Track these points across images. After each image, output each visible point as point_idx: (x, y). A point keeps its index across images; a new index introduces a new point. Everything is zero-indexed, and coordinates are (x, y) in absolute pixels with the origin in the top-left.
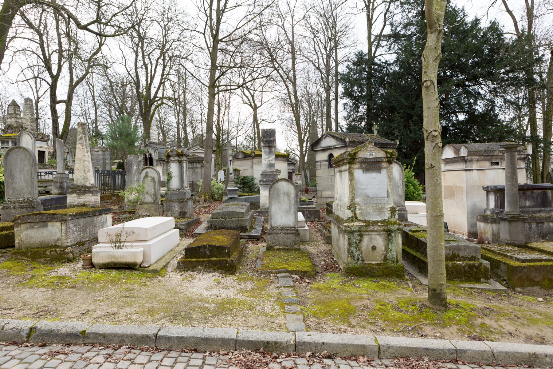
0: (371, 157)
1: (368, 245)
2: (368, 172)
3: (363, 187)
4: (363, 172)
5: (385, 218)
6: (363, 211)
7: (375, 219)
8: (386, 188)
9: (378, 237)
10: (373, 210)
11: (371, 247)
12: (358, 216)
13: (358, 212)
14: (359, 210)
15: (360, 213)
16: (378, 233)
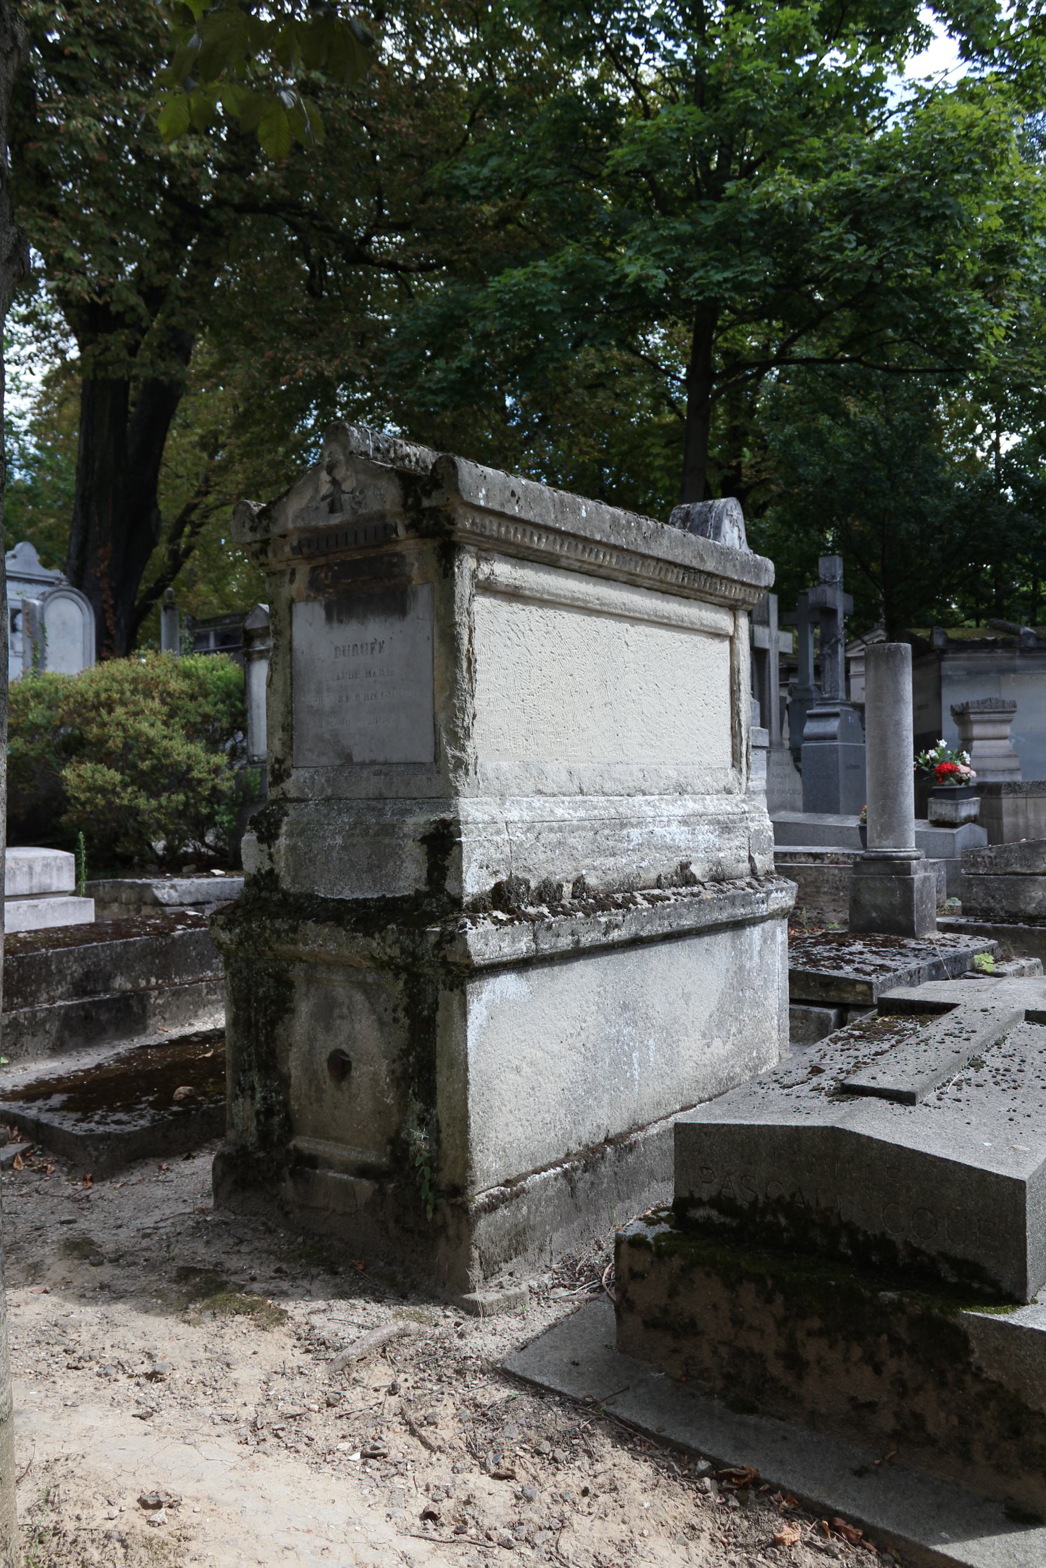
0: (336, 519)
4: (329, 618)
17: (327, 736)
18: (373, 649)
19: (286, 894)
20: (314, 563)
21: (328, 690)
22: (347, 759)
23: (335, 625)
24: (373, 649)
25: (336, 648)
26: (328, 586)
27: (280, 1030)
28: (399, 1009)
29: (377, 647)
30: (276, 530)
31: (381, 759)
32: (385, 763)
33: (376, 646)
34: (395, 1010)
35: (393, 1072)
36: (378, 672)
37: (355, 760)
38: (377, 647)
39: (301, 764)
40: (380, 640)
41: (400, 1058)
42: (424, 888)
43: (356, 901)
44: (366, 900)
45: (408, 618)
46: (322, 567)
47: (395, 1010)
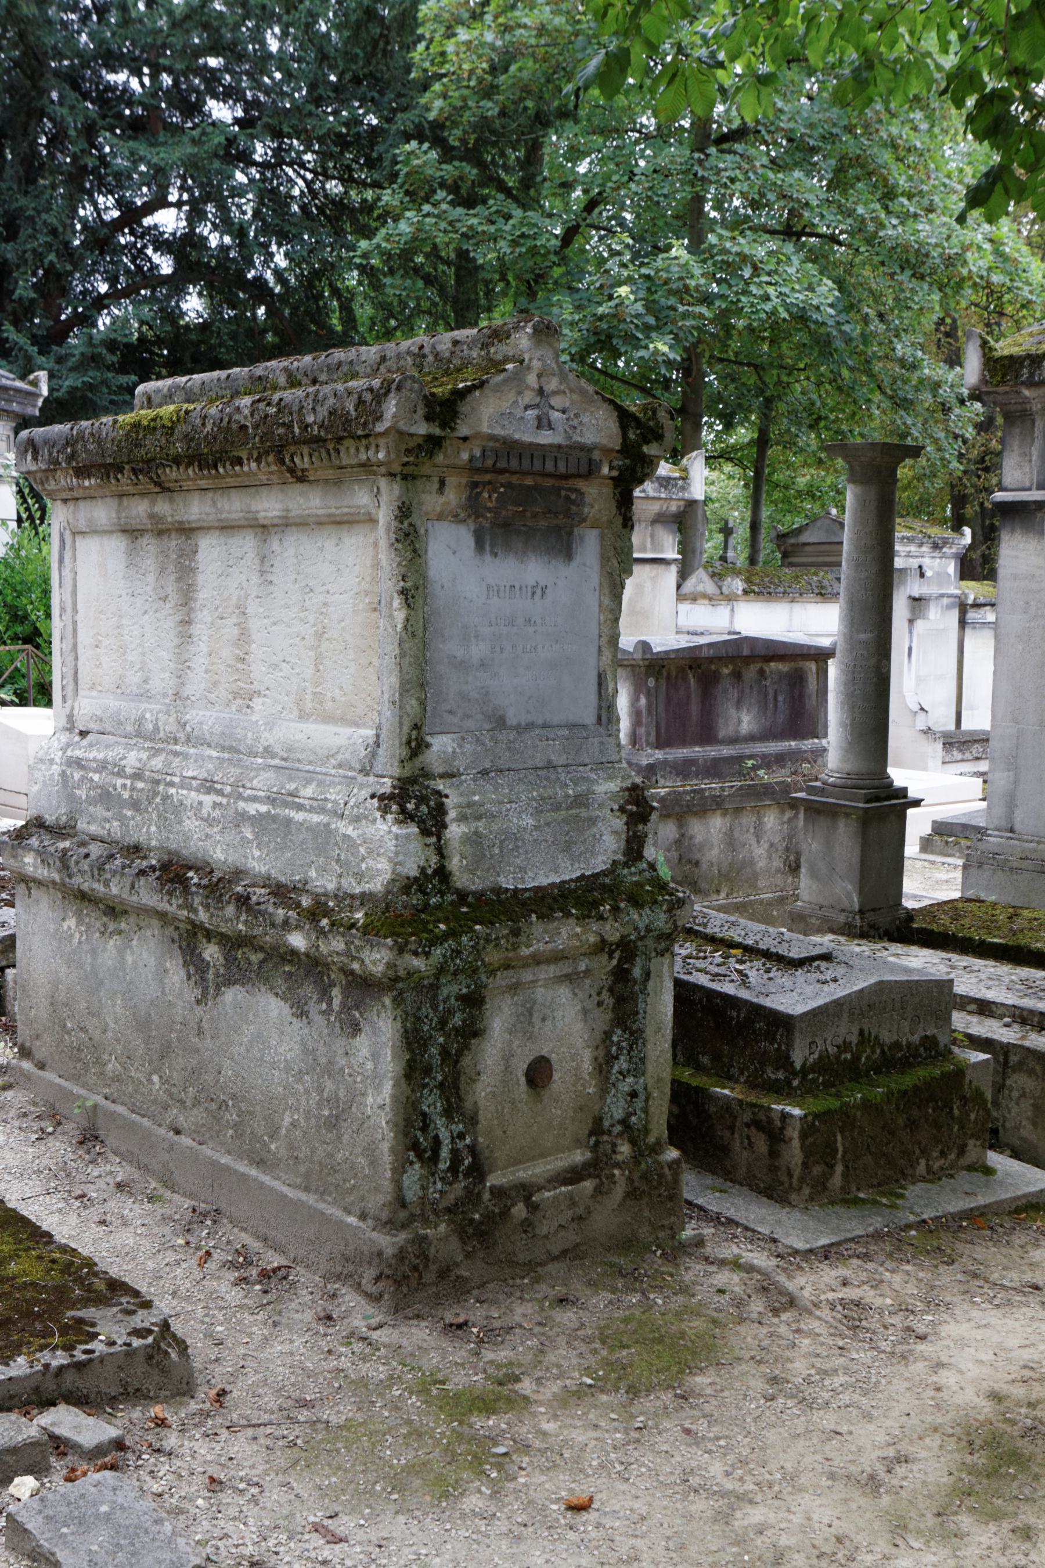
0: (545, 438)
1: (507, 1058)
2: (508, 547)
3: (478, 651)
4: (480, 546)
5: (599, 863)
6: (481, 825)
7: (545, 879)
8: (592, 661)
9: (563, 993)
10: (538, 812)
11: (521, 1067)
12: (454, 863)
13: (455, 831)
14: (462, 818)
15: (466, 840)
16: (565, 968)
17: (474, 695)
18: (533, 593)
19: (462, 896)
20: (477, 478)
21: (476, 637)
22: (500, 722)
23: (488, 558)
24: (533, 593)
25: (489, 587)
26: (489, 510)
27: (466, 1061)
28: (604, 992)
29: (539, 592)
30: (463, 430)
31: (540, 721)
32: (545, 726)
33: (539, 591)
34: (599, 994)
35: (596, 1059)
36: (539, 622)
37: (509, 722)
38: (539, 592)
39: (438, 729)
40: (542, 584)
41: (604, 1041)
42: (620, 857)
43: (553, 885)
44: (563, 882)
45: (574, 564)
46: (485, 484)
47: (599, 994)
